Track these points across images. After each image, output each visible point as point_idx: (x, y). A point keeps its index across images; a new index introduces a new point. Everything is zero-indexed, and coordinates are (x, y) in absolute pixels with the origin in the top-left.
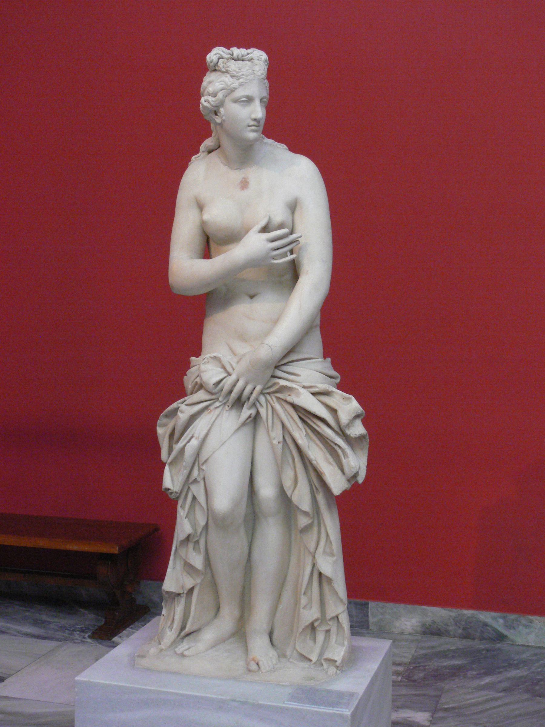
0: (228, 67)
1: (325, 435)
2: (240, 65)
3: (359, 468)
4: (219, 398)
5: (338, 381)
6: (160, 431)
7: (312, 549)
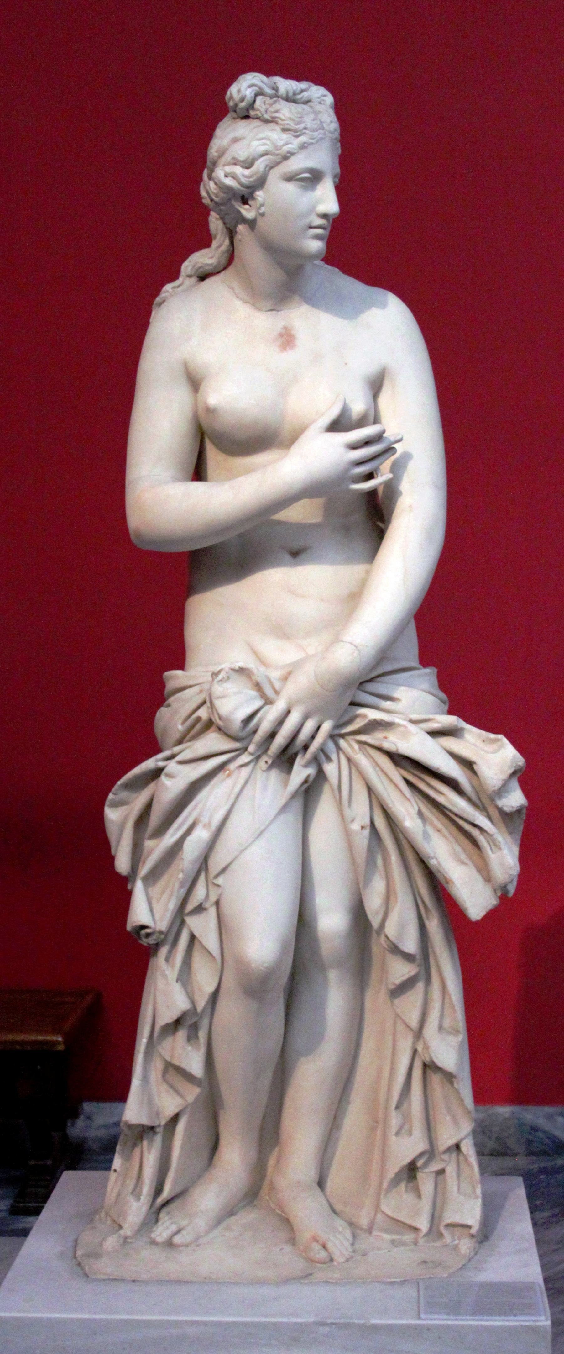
0: (277, 111)
1: (455, 810)
6: (112, 815)
7: (414, 1023)
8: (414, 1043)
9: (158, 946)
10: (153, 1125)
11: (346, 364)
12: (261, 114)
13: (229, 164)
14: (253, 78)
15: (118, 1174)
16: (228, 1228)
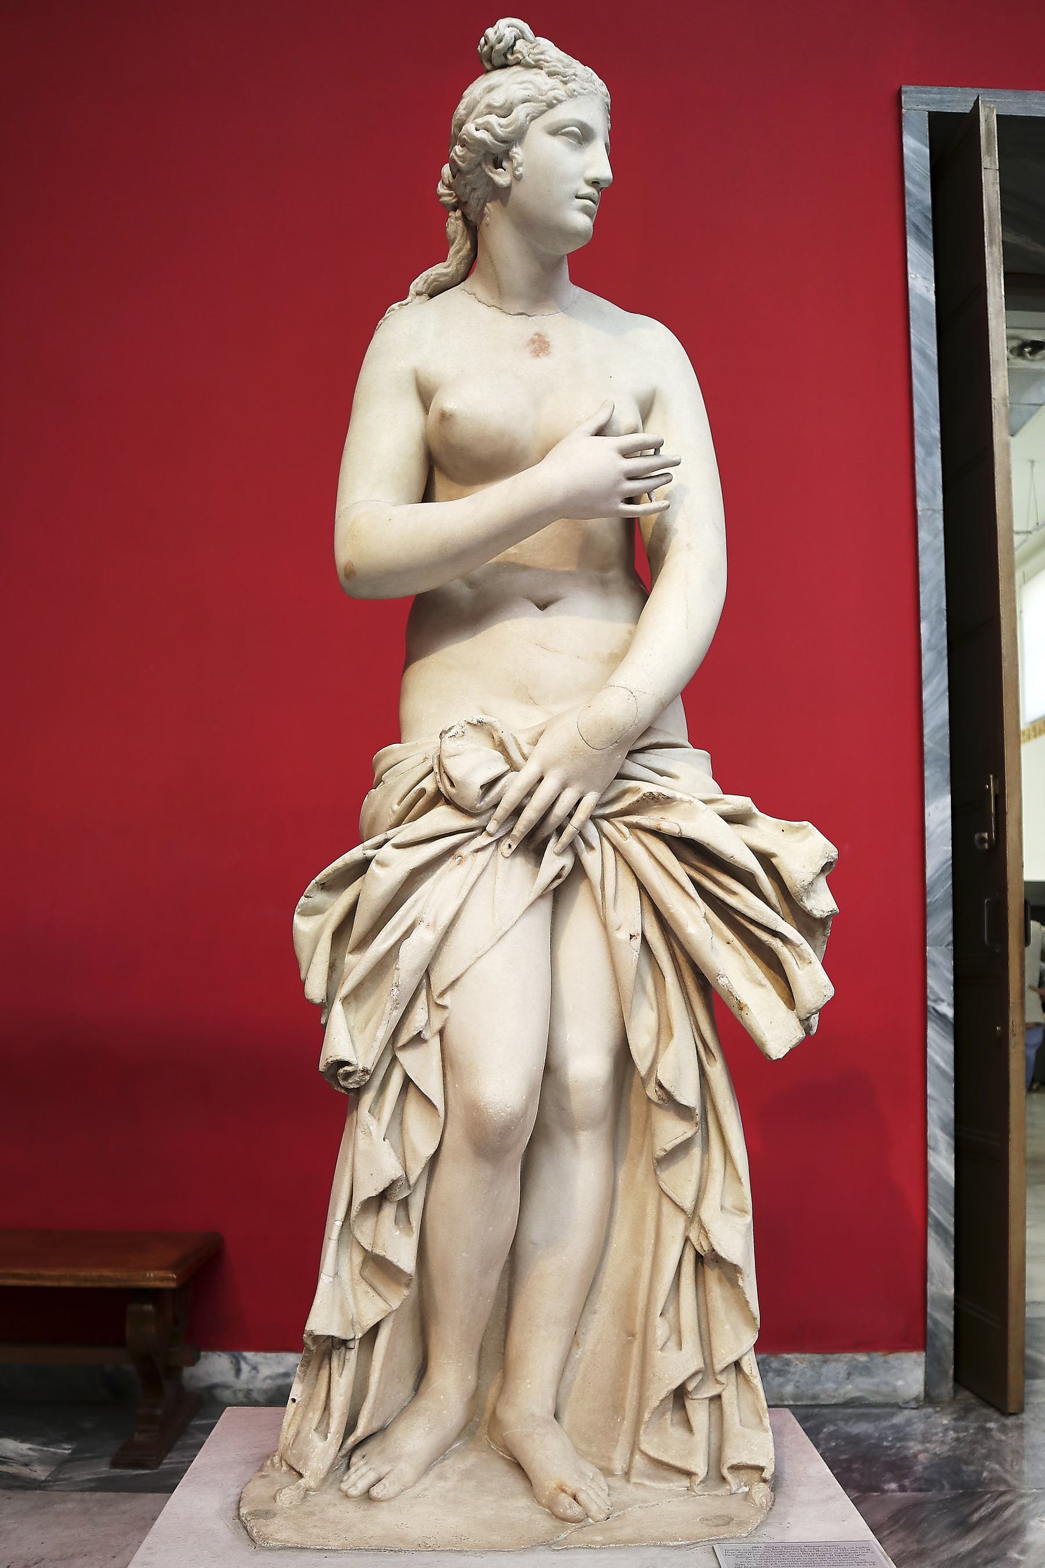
0: (542, 53)
8: (687, 1229)
9: (359, 1092)
10: (344, 1337)
13: (481, 115)
16: (442, 1477)
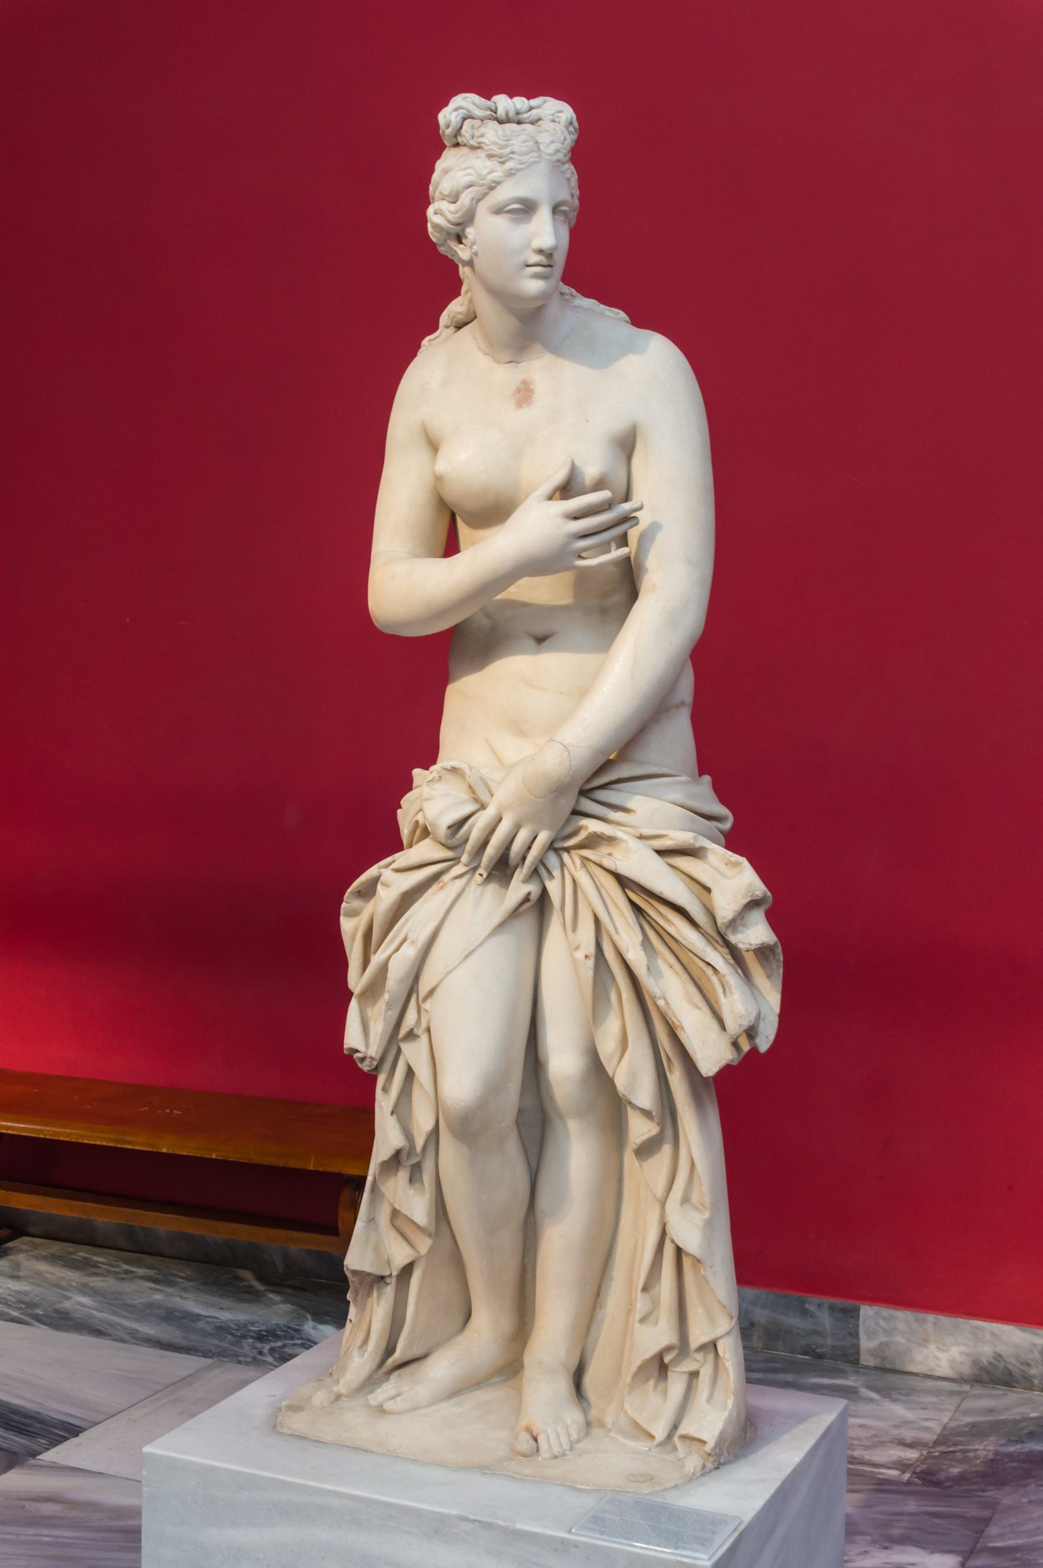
0: (482, 136)
2: (508, 132)
3: (758, 1017)
4: (460, 857)
5: (727, 825)
7: (660, 1192)
10: (377, 1272)
11: (587, 421)
12: (466, 139)
14: (464, 99)
15: (353, 1325)
